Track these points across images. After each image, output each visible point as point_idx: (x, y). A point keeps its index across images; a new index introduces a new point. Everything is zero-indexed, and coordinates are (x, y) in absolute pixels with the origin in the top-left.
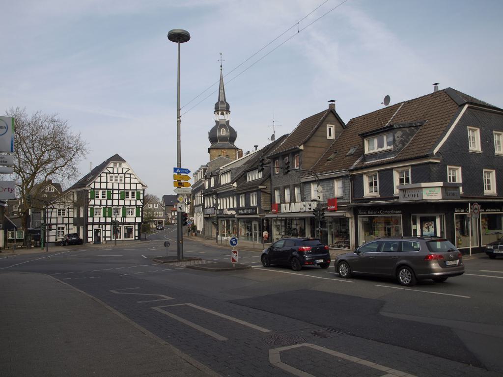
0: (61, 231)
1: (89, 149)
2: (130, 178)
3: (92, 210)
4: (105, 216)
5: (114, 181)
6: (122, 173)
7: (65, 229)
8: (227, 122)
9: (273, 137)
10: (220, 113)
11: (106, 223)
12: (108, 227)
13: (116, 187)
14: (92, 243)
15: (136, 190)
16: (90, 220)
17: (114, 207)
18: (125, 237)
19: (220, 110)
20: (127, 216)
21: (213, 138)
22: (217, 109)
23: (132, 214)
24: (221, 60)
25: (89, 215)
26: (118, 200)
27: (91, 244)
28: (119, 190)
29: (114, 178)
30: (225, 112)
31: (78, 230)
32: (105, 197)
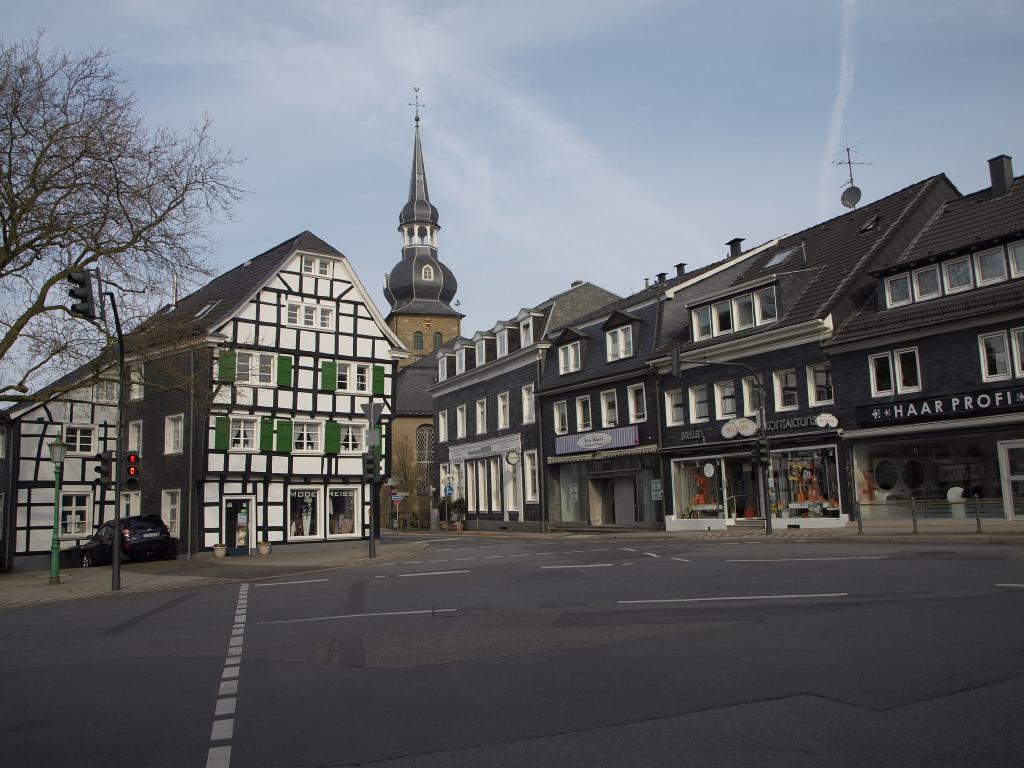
0: (74, 508)
1: (237, 185)
2: (355, 316)
3: (223, 424)
4: (267, 452)
5: (300, 323)
6: (330, 298)
7: (90, 501)
8: (434, 252)
9: (852, 194)
10: (416, 228)
11: (268, 477)
12: (276, 491)
14: (221, 552)
15: (373, 360)
16: (215, 463)
17: (299, 418)
18: (332, 532)
19: (418, 222)
20: (343, 451)
21: (400, 289)
22: (407, 219)
23: (355, 446)
24: (417, 105)
25: (212, 445)
26: (315, 392)
27: (215, 556)
28: (316, 355)
29: (301, 314)
30: (428, 228)
31: (151, 504)
32: (268, 379)
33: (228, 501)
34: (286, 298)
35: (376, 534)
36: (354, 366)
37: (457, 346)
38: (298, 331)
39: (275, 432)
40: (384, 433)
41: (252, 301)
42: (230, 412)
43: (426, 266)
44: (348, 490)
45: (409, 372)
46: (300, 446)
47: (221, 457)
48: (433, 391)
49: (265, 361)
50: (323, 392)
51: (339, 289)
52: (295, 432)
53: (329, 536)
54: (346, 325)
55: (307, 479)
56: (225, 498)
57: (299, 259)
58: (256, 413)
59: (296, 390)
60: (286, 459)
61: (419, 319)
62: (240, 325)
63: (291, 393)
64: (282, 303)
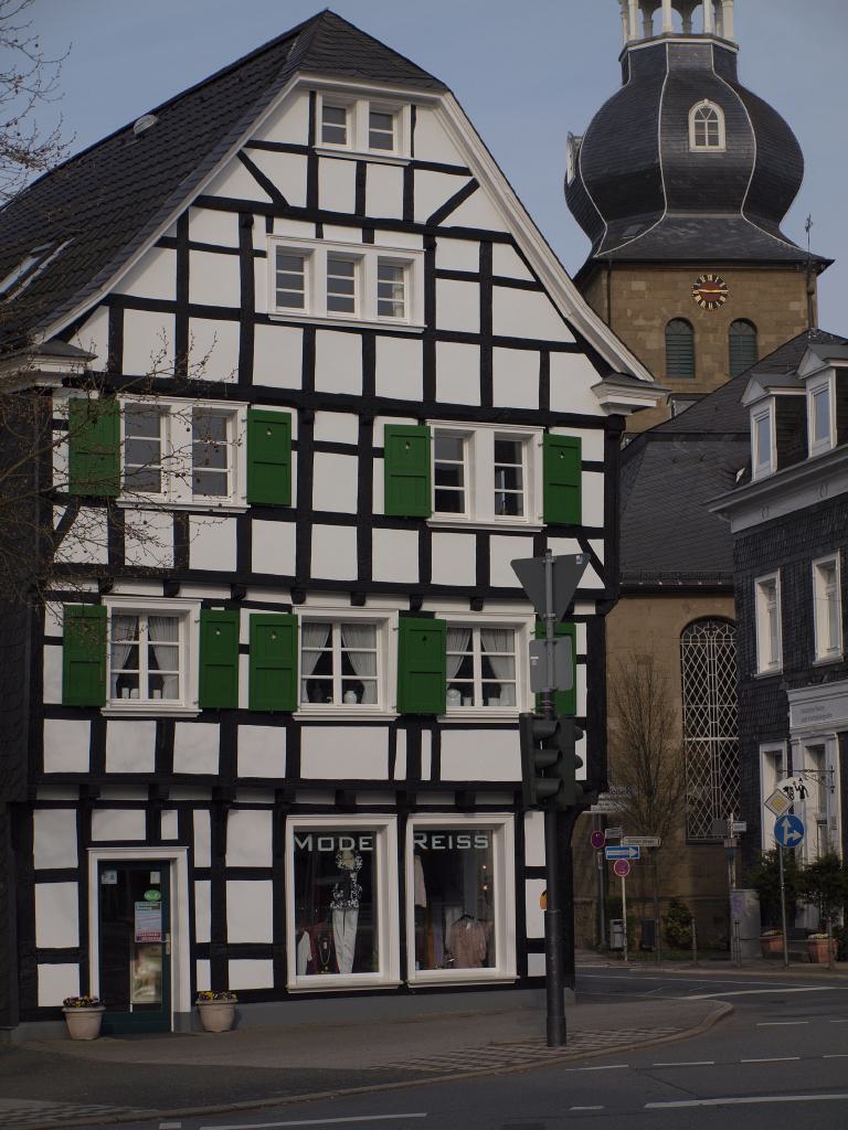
4: (220, 712)
5: (315, 305)
6: (406, 225)
8: (726, 57)
12: (250, 836)
13: (339, 370)
14: (85, 1023)
15: (543, 416)
16: (65, 747)
18: (423, 964)
20: (455, 709)
23: (492, 692)
25: (53, 693)
26: (364, 522)
27: (68, 1036)
28: (367, 406)
29: (316, 276)
32: (219, 486)
33: (104, 866)
34: (269, 229)
35: (565, 967)
36: (484, 438)
37: (810, 364)
38: (310, 330)
39: (244, 649)
40: (582, 649)
41: (164, 243)
42: (106, 590)
43: (698, 106)
44: (470, 832)
45: (653, 449)
46: (320, 692)
47: (81, 730)
48: (733, 511)
49: (208, 432)
50: (391, 521)
51: (432, 192)
52: (307, 648)
53: (416, 976)
54: (458, 306)
55: (345, 795)
56: (94, 857)
57: (304, 101)
58: (185, 592)
59: (306, 518)
60: (279, 734)
61: (682, 279)
62: (129, 314)
63: (289, 529)
64: (256, 246)
